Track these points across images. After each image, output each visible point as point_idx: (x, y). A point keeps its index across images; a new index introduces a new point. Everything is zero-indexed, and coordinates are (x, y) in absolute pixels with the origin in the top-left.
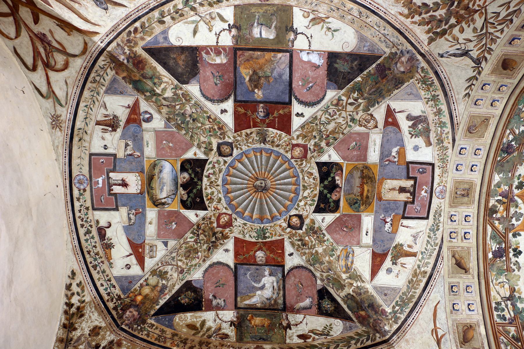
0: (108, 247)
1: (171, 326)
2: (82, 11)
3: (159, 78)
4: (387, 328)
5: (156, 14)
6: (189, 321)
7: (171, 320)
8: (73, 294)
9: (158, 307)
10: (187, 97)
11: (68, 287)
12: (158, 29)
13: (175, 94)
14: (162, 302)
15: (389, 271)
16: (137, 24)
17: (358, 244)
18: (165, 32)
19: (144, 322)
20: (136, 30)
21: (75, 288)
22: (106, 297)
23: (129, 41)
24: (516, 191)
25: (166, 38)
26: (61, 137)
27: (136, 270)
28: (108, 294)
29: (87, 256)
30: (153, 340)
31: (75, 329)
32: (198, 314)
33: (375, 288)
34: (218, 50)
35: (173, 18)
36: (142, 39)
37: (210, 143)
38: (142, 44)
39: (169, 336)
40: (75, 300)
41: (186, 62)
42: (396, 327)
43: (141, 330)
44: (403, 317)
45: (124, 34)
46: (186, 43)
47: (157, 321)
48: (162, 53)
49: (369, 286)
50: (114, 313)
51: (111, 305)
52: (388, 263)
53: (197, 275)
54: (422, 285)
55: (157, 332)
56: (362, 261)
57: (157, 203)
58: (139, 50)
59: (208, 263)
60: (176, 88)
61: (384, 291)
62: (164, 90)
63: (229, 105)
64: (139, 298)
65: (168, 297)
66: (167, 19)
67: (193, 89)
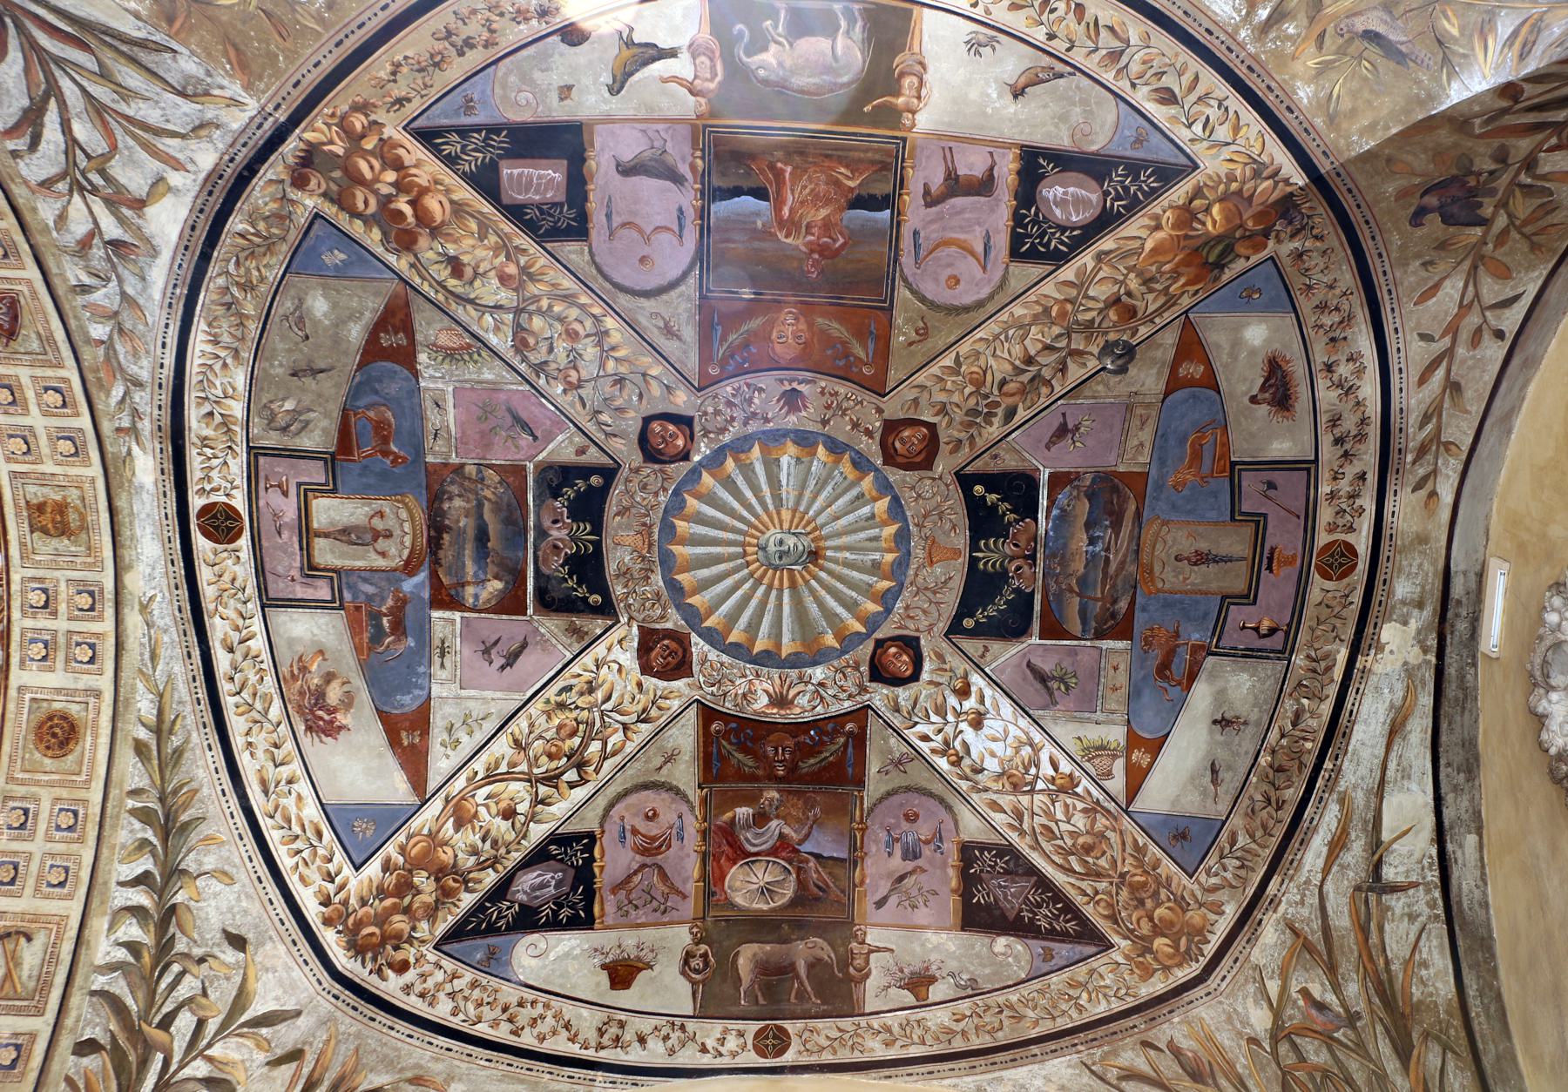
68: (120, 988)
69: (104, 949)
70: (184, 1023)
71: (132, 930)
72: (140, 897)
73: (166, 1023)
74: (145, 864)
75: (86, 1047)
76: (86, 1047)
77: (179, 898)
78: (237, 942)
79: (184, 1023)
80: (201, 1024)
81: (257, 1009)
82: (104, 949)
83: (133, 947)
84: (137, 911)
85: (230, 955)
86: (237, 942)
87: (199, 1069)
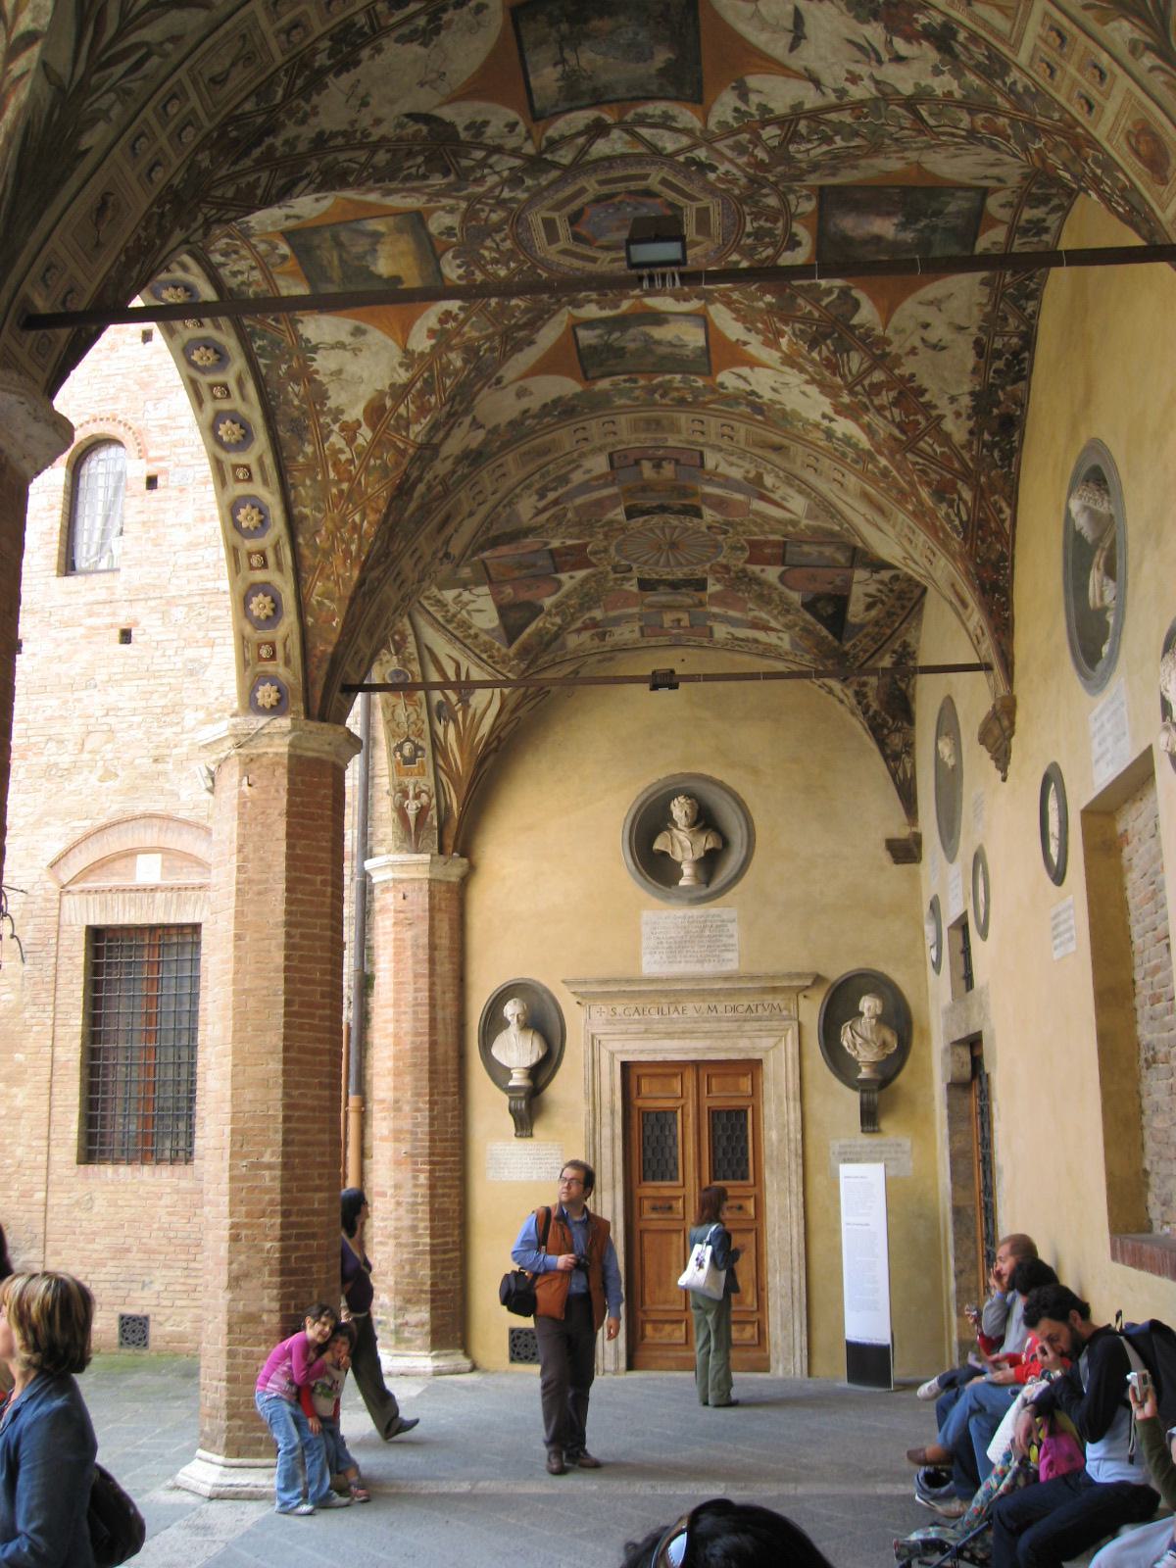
0: (756, 641)
1: (862, 626)
2: (483, 706)
3: (541, 629)
5: (468, 641)
6: (862, 607)
7: (854, 626)
9: (830, 637)
10: (557, 605)
12: (484, 637)
13: (557, 614)
14: (825, 632)
16: (484, 656)
18: (487, 632)
19: (846, 654)
20: (490, 657)
23: (504, 662)
24: (642, 382)
25: (493, 630)
26: (620, 655)
30: (876, 647)
32: (853, 598)
34: (495, 594)
35: (470, 628)
36: (499, 649)
37: (616, 579)
38: (504, 650)
39: (876, 630)
41: (514, 617)
43: (856, 657)
45: (498, 667)
46: (495, 615)
47: (850, 639)
48: (510, 632)
53: (796, 597)
55: (864, 641)
57: (701, 604)
58: (512, 651)
59: (779, 586)
60: (549, 614)
62: (553, 624)
63: (563, 577)
65: (819, 626)
66: (472, 632)
67: (548, 602)
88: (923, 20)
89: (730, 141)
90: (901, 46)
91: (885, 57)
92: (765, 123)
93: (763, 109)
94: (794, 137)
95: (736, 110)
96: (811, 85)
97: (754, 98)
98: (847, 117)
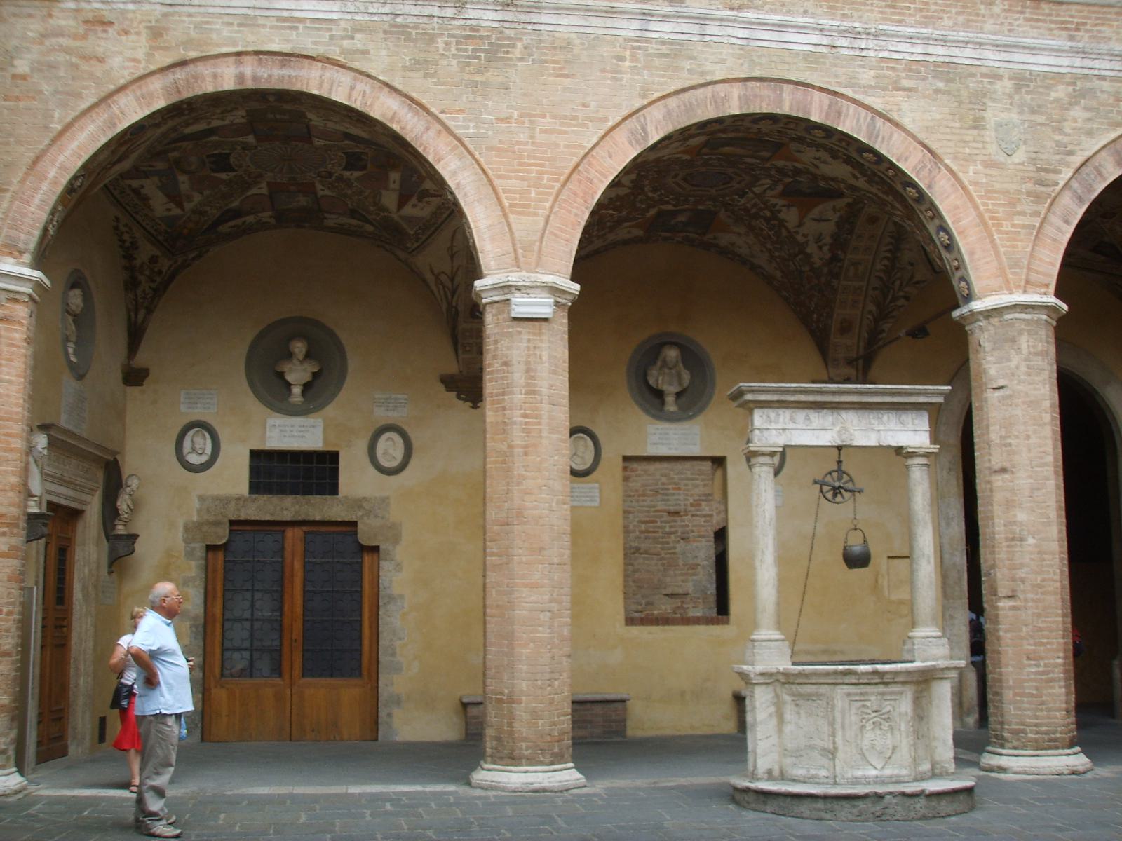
4: (408, 245)
8: (122, 233)
11: (116, 228)
15: (414, 206)
17: (386, 188)
21: (123, 229)
22: (155, 233)
27: (176, 211)
28: (156, 230)
29: (128, 208)
31: (135, 259)
33: (401, 217)
40: (126, 237)
42: (416, 245)
44: (424, 238)
49: (395, 216)
50: (166, 244)
51: (161, 238)
52: (414, 200)
54: (445, 216)
56: (389, 199)
61: (409, 220)
64: (185, 231)
68: (882, 275)
69: (879, 266)
70: (898, 283)
71: (886, 262)
72: (888, 255)
73: (893, 283)
74: (890, 247)
75: (874, 289)
76: (874, 289)
77: (899, 255)
78: (912, 264)
79: (898, 283)
80: (901, 283)
81: (915, 280)
82: (879, 266)
83: (885, 265)
84: (886, 258)
85: (910, 268)
86: (912, 264)
87: (901, 294)
88: (839, 253)
89: (759, 202)
90: (826, 249)
91: (820, 244)
92: (771, 211)
93: (780, 211)
94: (767, 220)
95: (776, 204)
96: (797, 224)
97: (784, 209)
98: (784, 233)
